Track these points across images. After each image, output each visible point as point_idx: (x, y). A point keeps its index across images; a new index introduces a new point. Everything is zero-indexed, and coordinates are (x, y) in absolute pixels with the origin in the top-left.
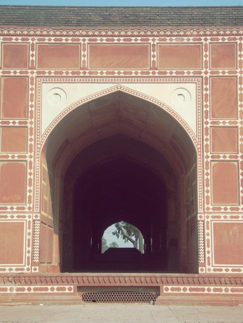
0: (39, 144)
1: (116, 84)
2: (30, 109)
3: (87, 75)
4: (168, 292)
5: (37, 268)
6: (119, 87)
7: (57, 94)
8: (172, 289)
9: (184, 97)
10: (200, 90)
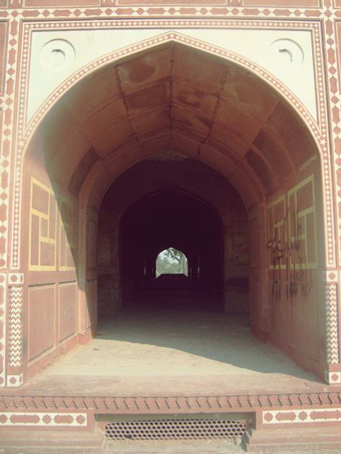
0: (23, 140)
1: (166, 31)
2: (8, 77)
3: (114, 15)
4: (271, 422)
5: (17, 377)
6: (172, 36)
7: (58, 51)
8: (279, 417)
9: (291, 56)
10: (319, 42)
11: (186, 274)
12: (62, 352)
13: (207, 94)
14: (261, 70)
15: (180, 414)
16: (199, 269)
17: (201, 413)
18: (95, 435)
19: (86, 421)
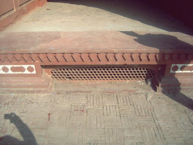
12: (23, 13)
17: (125, 65)
18: (43, 80)
19: (35, 71)
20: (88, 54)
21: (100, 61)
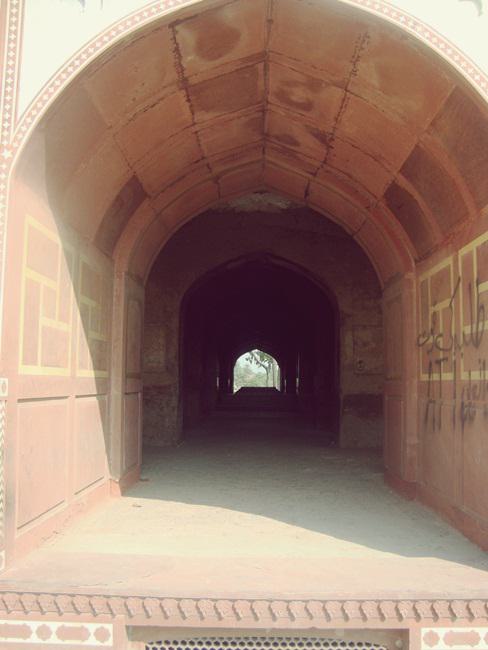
0: (9, 148)
11: (278, 387)
13: (326, 83)
14: (427, 30)
15: (274, 630)
16: (297, 385)
17: (313, 630)
19: (111, 639)
20: (231, 604)
21: (256, 619)
